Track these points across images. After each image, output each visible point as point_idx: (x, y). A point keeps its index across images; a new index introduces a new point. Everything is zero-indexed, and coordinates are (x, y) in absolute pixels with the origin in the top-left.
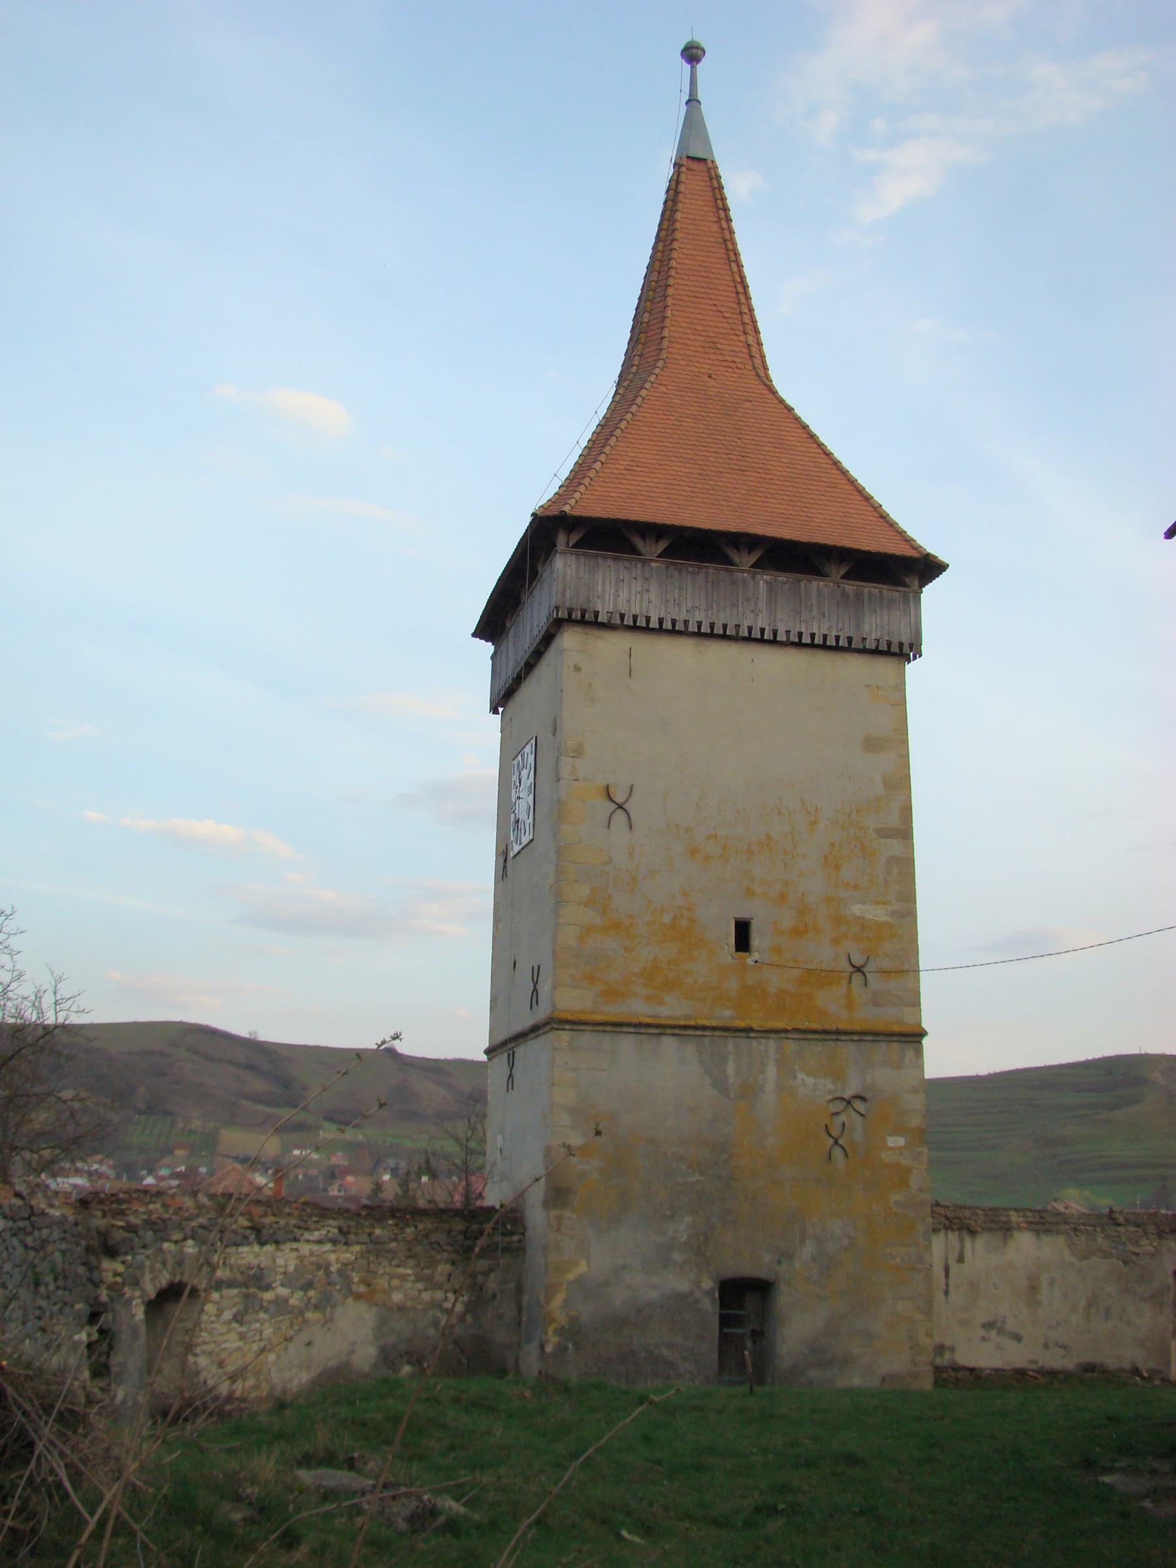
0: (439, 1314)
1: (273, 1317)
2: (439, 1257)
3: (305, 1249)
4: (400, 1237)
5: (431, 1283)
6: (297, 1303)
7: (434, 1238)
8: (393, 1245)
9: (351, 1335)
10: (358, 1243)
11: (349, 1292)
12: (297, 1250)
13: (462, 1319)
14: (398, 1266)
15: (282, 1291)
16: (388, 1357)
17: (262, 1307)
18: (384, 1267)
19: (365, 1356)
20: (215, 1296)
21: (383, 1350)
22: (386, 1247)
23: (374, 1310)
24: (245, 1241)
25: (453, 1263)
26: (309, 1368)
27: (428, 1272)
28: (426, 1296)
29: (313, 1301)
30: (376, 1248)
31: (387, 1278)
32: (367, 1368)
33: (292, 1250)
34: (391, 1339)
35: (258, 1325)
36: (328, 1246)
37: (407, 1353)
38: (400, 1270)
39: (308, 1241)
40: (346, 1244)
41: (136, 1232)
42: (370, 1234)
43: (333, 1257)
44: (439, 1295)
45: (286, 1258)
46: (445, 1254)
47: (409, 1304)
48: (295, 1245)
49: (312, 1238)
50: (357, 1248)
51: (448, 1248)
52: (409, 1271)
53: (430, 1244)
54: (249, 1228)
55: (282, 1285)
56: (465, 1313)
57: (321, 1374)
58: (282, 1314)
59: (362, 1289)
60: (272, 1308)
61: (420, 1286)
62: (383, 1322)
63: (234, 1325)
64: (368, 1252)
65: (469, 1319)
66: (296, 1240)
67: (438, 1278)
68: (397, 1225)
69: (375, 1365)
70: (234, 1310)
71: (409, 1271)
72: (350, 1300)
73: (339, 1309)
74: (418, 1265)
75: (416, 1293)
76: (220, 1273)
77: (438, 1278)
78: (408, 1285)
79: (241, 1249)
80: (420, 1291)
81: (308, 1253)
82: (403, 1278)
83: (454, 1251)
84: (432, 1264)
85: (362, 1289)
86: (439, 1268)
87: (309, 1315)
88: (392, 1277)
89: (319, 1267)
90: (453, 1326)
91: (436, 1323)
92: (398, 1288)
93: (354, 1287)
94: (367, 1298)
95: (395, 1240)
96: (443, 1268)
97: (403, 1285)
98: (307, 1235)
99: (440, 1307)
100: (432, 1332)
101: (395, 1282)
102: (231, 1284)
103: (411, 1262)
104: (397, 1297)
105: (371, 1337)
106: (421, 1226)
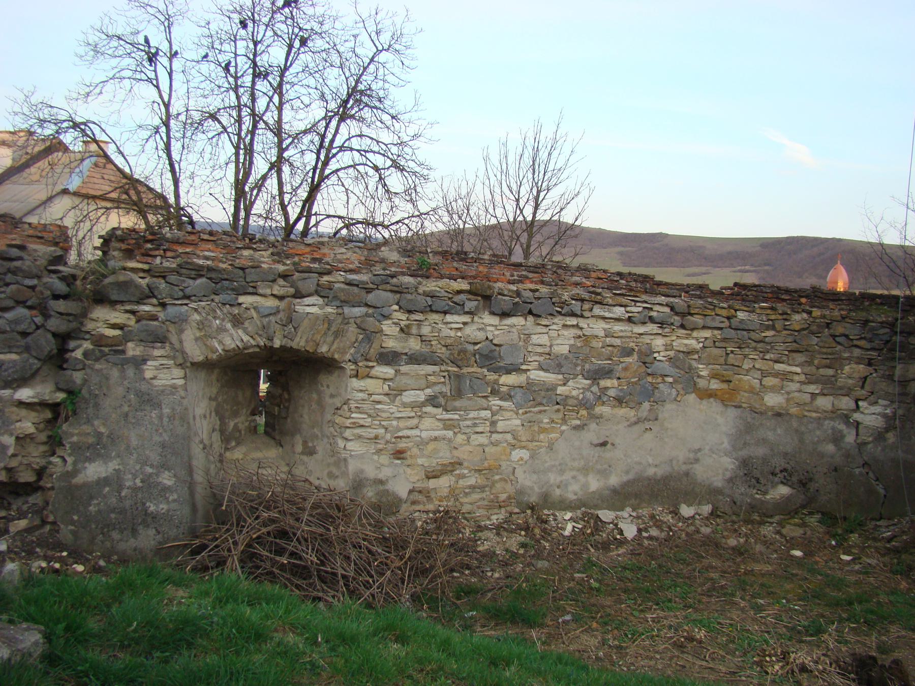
0: (842, 427)
1: (519, 406)
2: (846, 355)
3: (598, 328)
4: (779, 325)
5: (830, 387)
6: (574, 393)
7: (839, 329)
8: (770, 333)
9: (697, 437)
10: (704, 327)
11: (696, 389)
12: (577, 326)
13: (880, 436)
14: (776, 361)
15: (536, 375)
16: (750, 473)
17: (494, 392)
18: (752, 361)
19: (717, 467)
20: (387, 371)
21: (745, 463)
22: (753, 335)
23: (732, 413)
24: (458, 308)
25: (870, 364)
26: (604, 473)
27: (830, 372)
28: (824, 403)
29: (612, 393)
30: (741, 338)
31: (758, 375)
32: (720, 485)
33: (565, 326)
34: (760, 451)
35: (486, 414)
36: (652, 328)
37: (785, 470)
38: (778, 367)
39: (604, 318)
40: (682, 326)
41: (164, 277)
42: (728, 318)
43: (659, 342)
44: (846, 403)
45: (556, 336)
46: (857, 352)
47: (794, 410)
48: (573, 321)
49: (607, 315)
50: (707, 334)
51: (862, 343)
52: (798, 370)
53: (834, 336)
54: (469, 292)
55: (541, 368)
56: (887, 430)
57: (625, 485)
58: (541, 404)
59: (715, 385)
60: (519, 395)
61: (813, 388)
62: (749, 428)
63: (429, 409)
64: (724, 340)
65: (891, 437)
66: (573, 314)
67: (841, 381)
68: (772, 308)
69: (731, 480)
70: (429, 391)
71: (798, 370)
72: (692, 397)
73: (669, 406)
74: (810, 363)
75: (807, 398)
76: (391, 344)
77: (841, 381)
78: (794, 386)
79: (449, 318)
80: (813, 396)
81: (602, 334)
82: (785, 377)
83: (873, 349)
84: (835, 363)
85: (715, 385)
86: (847, 368)
87: (603, 410)
88: (765, 374)
89: (628, 352)
90: (865, 444)
91: (837, 439)
92: (773, 389)
93: (702, 383)
94: (726, 399)
95: (773, 328)
96: (852, 371)
97: (784, 387)
98: (597, 310)
99: (846, 418)
100: (830, 448)
101: (770, 381)
102: (415, 359)
103: (800, 358)
104: (773, 400)
105: (726, 445)
106: (816, 312)
